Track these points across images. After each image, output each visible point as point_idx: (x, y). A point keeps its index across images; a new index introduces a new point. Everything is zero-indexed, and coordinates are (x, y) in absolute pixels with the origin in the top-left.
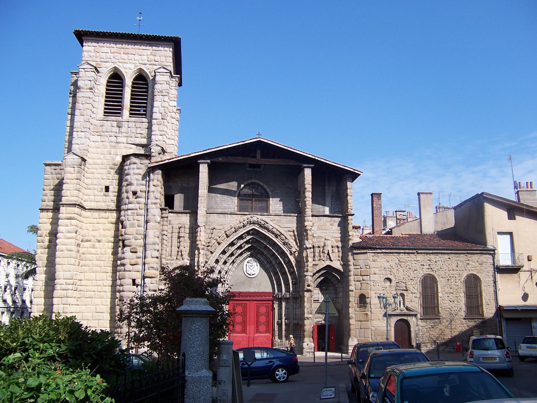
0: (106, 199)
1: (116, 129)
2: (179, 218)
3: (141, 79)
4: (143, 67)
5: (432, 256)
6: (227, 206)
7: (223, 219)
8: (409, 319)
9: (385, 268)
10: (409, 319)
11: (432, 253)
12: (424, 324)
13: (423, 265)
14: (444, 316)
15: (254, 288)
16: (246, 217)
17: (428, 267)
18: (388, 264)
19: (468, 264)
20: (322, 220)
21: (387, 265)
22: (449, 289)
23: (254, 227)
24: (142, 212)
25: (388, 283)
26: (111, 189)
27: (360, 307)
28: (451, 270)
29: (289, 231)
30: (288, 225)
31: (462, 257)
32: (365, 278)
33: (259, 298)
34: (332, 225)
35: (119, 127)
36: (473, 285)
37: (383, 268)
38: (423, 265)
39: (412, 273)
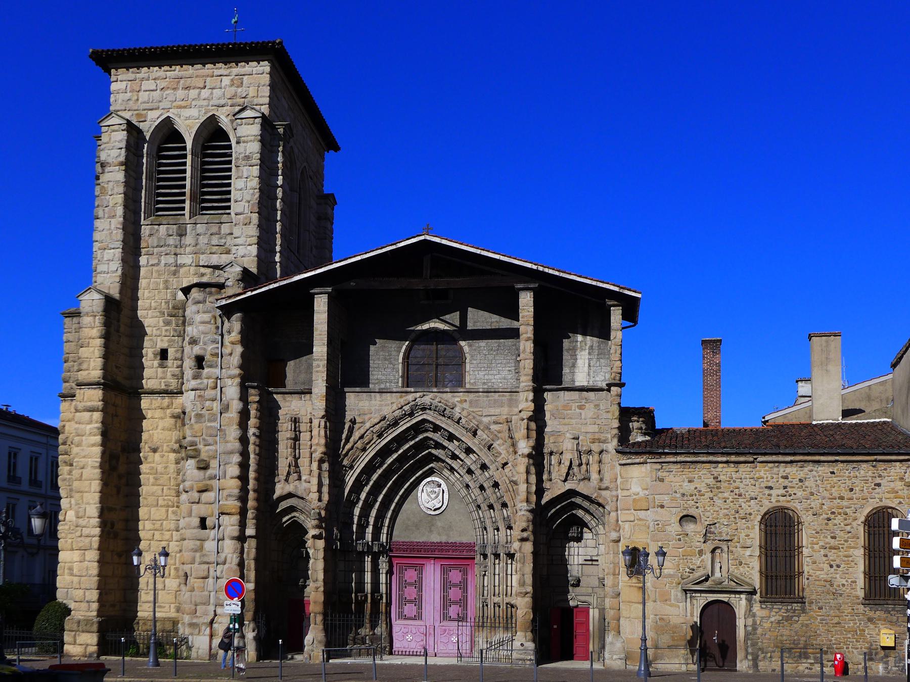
2: (287, 404)
5: (791, 470)
6: (383, 378)
7: (367, 403)
8: (732, 599)
9: (683, 495)
10: (732, 599)
11: (792, 462)
12: (764, 613)
13: (771, 488)
14: (814, 597)
15: (439, 534)
16: (410, 397)
17: (782, 491)
18: (692, 486)
19: (879, 485)
20: (561, 399)
22: (829, 540)
23: (425, 417)
30: (492, 411)
31: (865, 470)
33: (455, 554)
34: (581, 407)
37: (678, 495)
38: (771, 488)
39: (743, 505)
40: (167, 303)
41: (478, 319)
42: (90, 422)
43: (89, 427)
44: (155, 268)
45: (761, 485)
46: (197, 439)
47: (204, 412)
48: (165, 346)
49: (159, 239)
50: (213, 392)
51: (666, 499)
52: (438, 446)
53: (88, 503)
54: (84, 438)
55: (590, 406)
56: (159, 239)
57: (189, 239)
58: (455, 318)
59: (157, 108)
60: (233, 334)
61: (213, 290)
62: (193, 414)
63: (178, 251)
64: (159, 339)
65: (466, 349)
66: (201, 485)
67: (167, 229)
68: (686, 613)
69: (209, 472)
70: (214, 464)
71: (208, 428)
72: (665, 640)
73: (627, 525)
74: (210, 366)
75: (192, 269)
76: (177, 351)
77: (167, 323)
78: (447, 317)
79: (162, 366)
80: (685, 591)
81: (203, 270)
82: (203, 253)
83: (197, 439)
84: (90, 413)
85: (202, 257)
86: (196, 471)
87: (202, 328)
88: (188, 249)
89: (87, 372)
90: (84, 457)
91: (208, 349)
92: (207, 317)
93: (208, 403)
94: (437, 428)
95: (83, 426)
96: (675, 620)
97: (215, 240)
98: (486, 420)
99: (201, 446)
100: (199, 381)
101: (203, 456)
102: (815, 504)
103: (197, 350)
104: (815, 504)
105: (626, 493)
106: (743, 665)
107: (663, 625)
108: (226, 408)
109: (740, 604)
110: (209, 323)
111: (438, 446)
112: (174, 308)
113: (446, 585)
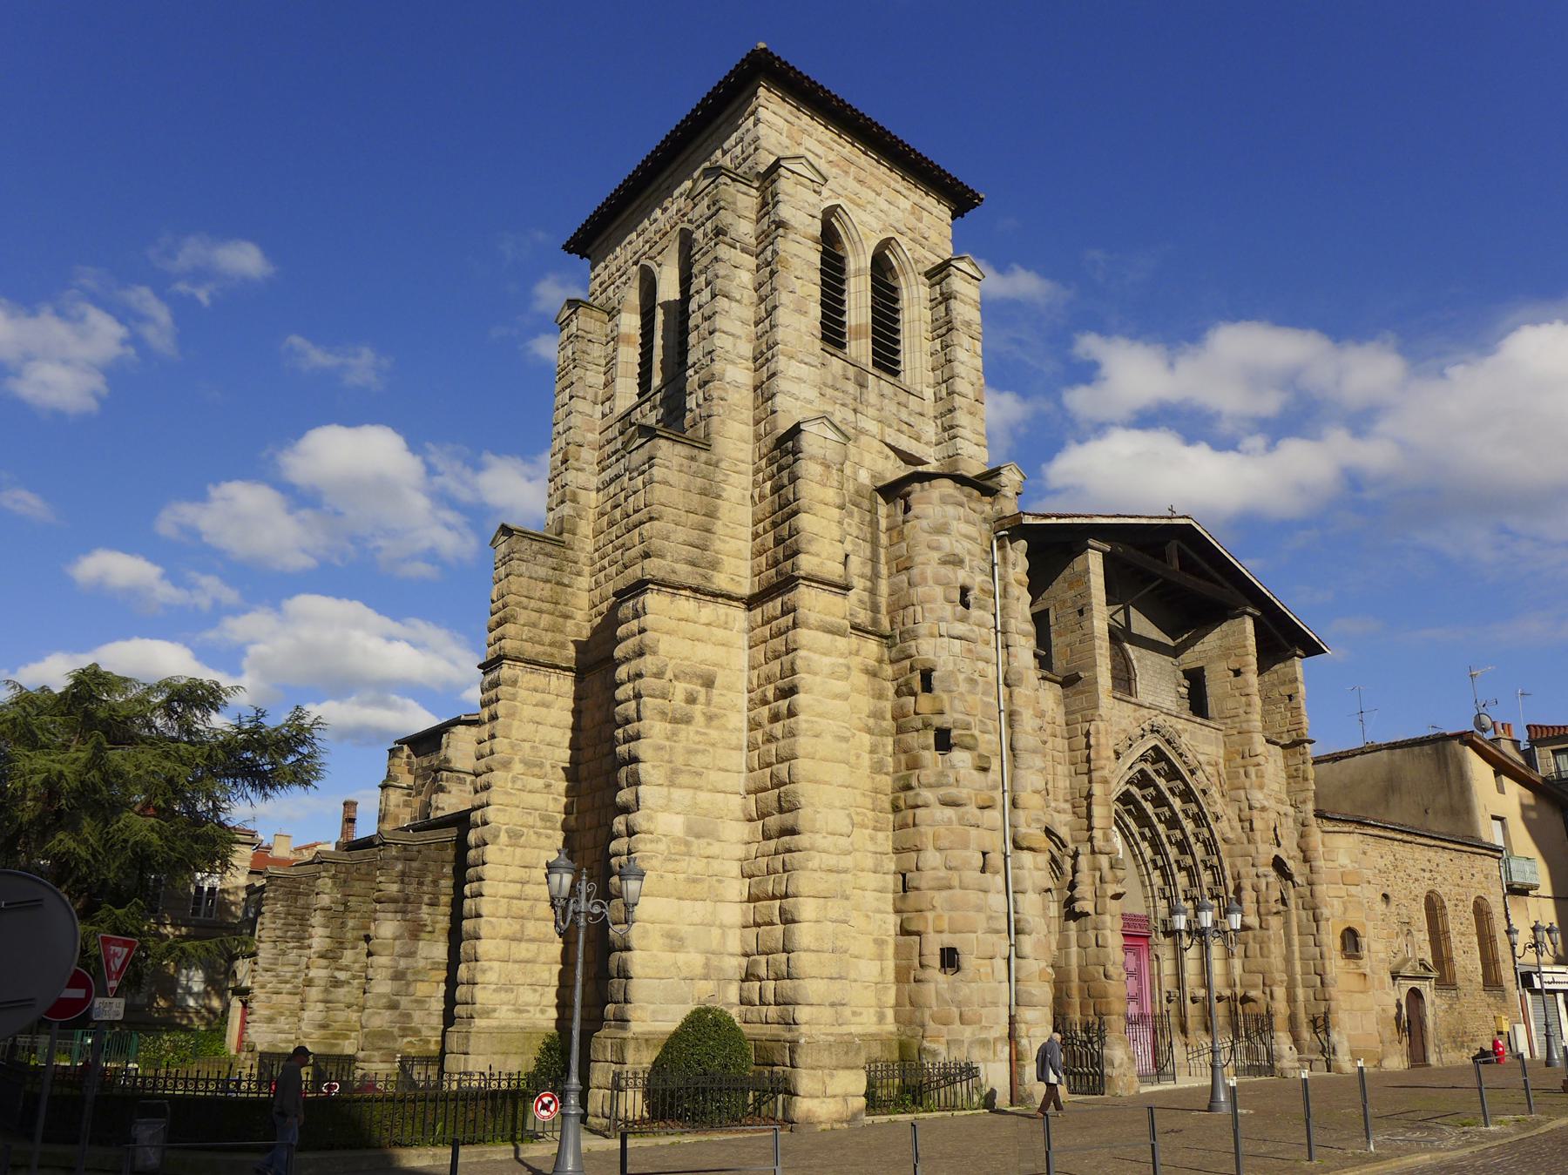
1: (851, 387)
21: (1381, 863)
27: (1348, 957)
29: (1209, 764)
32: (1353, 889)
43: (827, 660)
46: (970, 719)
47: (976, 676)
49: (834, 377)
50: (987, 649)
51: (1368, 874)
53: (830, 806)
54: (818, 679)
56: (834, 377)
57: (872, 396)
60: (1018, 569)
61: (976, 493)
62: (961, 677)
63: (860, 408)
67: (845, 369)
70: (995, 765)
73: (1336, 902)
75: (877, 444)
80: (1394, 978)
81: (887, 450)
82: (890, 426)
83: (970, 719)
84: (829, 636)
85: (887, 430)
86: (975, 773)
87: (967, 544)
88: (871, 412)
89: (816, 560)
90: (820, 715)
91: (978, 581)
93: (981, 665)
95: (816, 657)
97: (904, 416)
99: (976, 733)
101: (983, 749)
103: (962, 576)
105: (1330, 864)
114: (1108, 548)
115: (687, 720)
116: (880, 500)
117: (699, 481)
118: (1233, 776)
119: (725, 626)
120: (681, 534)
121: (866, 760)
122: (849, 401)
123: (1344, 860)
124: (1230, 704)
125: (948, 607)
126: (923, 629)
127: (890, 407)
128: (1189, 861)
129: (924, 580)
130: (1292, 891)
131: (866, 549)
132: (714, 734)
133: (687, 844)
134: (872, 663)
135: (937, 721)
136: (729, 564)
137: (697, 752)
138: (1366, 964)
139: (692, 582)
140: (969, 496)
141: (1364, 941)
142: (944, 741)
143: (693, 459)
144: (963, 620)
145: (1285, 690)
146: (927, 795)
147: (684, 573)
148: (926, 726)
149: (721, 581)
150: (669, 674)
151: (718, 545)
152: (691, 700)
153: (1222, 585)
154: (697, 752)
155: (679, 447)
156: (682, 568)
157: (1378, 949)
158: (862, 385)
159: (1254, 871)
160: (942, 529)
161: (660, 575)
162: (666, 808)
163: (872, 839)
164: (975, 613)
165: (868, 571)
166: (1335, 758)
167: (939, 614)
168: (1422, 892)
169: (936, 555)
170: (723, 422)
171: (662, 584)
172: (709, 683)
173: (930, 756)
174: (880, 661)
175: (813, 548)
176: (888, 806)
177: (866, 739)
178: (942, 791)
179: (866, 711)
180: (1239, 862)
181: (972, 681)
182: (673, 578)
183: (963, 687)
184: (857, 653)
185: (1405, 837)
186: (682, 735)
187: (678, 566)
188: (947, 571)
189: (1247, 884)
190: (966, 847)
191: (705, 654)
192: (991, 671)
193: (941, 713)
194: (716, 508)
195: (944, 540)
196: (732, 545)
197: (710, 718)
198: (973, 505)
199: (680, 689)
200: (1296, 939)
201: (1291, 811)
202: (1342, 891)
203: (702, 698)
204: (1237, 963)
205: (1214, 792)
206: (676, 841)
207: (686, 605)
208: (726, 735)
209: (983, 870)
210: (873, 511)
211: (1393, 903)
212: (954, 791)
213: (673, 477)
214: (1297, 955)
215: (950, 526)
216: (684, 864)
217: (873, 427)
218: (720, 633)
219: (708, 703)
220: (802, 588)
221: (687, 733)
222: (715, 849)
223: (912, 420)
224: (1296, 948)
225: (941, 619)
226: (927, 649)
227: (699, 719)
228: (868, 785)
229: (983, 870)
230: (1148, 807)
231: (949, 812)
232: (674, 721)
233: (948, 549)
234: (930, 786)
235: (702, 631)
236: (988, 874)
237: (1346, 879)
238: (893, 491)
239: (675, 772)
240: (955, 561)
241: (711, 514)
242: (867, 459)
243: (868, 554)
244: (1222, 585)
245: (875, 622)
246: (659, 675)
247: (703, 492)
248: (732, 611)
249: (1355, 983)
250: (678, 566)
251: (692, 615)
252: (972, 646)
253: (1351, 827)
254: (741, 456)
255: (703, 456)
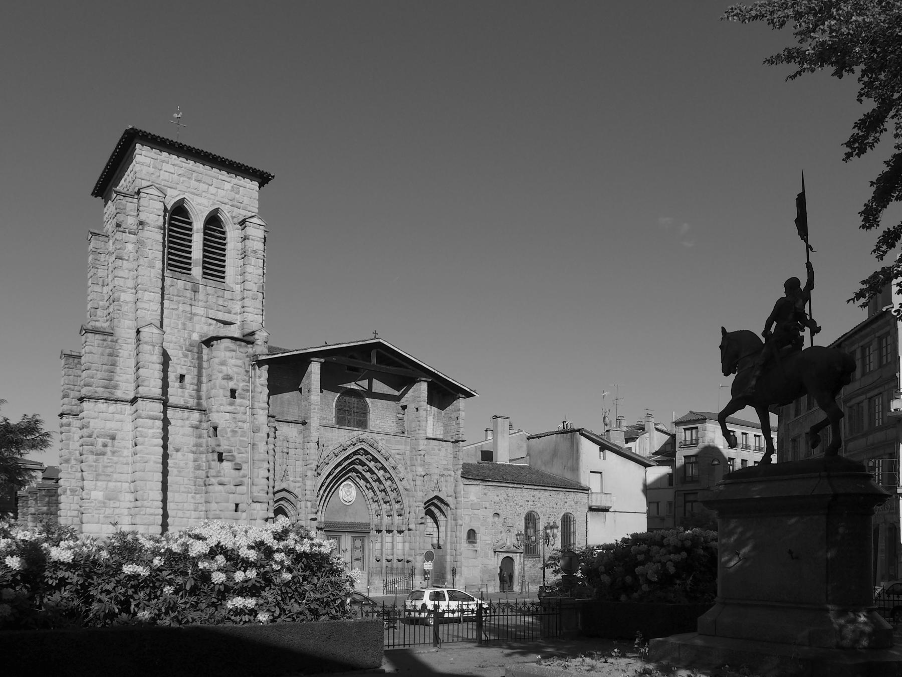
0: (183, 392)
1: (189, 294)
3: (214, 221)
4: (222, 207)
16: (355, 433)
21: (497, 499)
24: (248, 417)
25: (496, 519)
26: (188, 379)
27: (470, 542)
28: (550, 506)
32: (476, 512)
35: (195, 292)
36: (567, 521)
40: (185, 340)
41: (379, 387)
42: (152, 428)
43: (151, 431)
44: (174, 312)
45: (524, 499)
47: (237, 429)
48: (183, 373)
50: (244, 416)
51: (487, 505)
52: (362, 464)
53: (151, 490)
55: (443, 450)
57: (201, 296)
58: (365, 383)
59: (175, 189)
63: (193, 303)
64: (179, 367)
65: (370, 405)
66: (237, 481)
67: (185, 285)
68: (495, 563)
69: (242, 472)
70: (244, 466)
71: (241, 441)
72: (486, 577)
74: (243, 398)
75: (203, 319)
76: (193, 378)
77: (186, 356)
78: (360, 383)
79: (182, 387)
83: (233, 448)
84: (152, 421)
85: (210, 311)
87: (235, 369)
88: (200, 304)
89: (147, 389)
91: (240, 386)
92: (239, 362)
93: (240, 424)
94: (366, 453)
96: (490, 567)
97: (221, 302)
98: (393, 452)
99: (235, 454)
100: (233, 407)
101: (238, 460)
102: (544, 510)
103: (231, 385)
104: (544, 510)
106: (516, 588)
107: (485, 570)
108: (255, 430)
109: (517, 558)
110: (240, 367)
111: (362, 464)
112: (191, 345)
113: (354, 549)
114: (323, 360)
115: (104, 454)
116: (204, 346)
117: (108, 351)
118: (411, 459)
119: (121, 413)
120: (100, 375)
121: (191, 464)
122: (189, 302)
123: (473, 498)
124: (413, 425)
125: (224, 399)
126: (213, 410)
127: (212, 299)
128: (388, 499)
129: (215, 386)
130: (449, 512)
131: (195, 371)
132: (115, 459)
133: (104, 503)
134: (196, 423)
135: (218, 449)
136: (123, 385)
137: (107, 467)
138: (478, 546)
139: (106, 395)
140: (240, 345)
141: (478, 536)
142: (221, 459)
143: (104, 340)
144: (231, 404)
145: (456, 414)
146: (213, 480)
147: (101, 392)
148: (213, 451)
149: (119, 394)
150: (95, 436)
151: (117, 378)
152: (105, 445)
153: (407, 368)
154: (107, 467)
155: (97, 336)
156: (100, 390)
157: (484, 538)
158: (195, 291)
159: (415, 504)
160: (223, 363)
161: (89, 394)
162: (95, 489)
163: (193, 497)
164: (238, 401)
165: (195, 381)
166: (538, 437)
167: (220, 402)
168: (524, 512)
169: (221, 375)
170: (119, 321)
171: (90, 398)
172: (113, 438)
173: (215, 464)
174: (201, 421)
175: (146, 383)
176: (202, 484)
177: (191, 456)
178: (219, 479)
179: (192, 444)
180: (411, 499)
181: (234, 432)
182: (96, 395)
183: (229, 434)
184: (187, 419)
185: (516, 486)
186: (101, 460)
187: (98, 389)
188: (224, 382)
189: (412, 510)
190: (227, 502)
191: (110, 426)
192: (246, 426)
193: (219, 446)
194: (116, 362)
195: (224, 368)
196: (125, 377)
197: (113, 453)
198: (241, 350)
199: (100, 441)
200: (449, 533)
201: (453, 473)
202: (470, 512)
203: (110, 444)
204: (407, 545)
205: (400, 468)
206: (100, 502)
207: (102, 406)
208: (121, 459)
209: (236, 511)
210: (200, 352)
211: (502, 517)
212: (222, 479)
213: (94, 350)
214: (449, 540)
215: (229, 361)
216: (102, 511)
217: (200, 311)
218: (117, 416)
219: (113, 446)
220: (139, 402)
221: (105, 459)
222: (117, 505)
223: (226, 304)
224: (449, 538)
225: (221, 405)
226: (215, 417)
227: (109, 453)
228: (191, 475)
229: (236, 511)
230: (368, 475)
231: (221, 487)
232: (97, 454)
233: (225, 373)
234: (214, 477)
235: (109, 416)
236: (239, 513)
237: (474, 507)
238: (208, 342)
239: (98, 475)
240: (229, 378)
241: (114, 364)
242: (198, 327)
243: (196, 373)
244: (407, 368)
245: (199, 404)
246: (90, 436)
247: (110, 355)
248: (123, 407)
249: (471, 554)
250: (98, 389)
251: (104, 410)
252: (236, 415)
253: (479, 482)
254: (128, 336)
255: (110, 338)
